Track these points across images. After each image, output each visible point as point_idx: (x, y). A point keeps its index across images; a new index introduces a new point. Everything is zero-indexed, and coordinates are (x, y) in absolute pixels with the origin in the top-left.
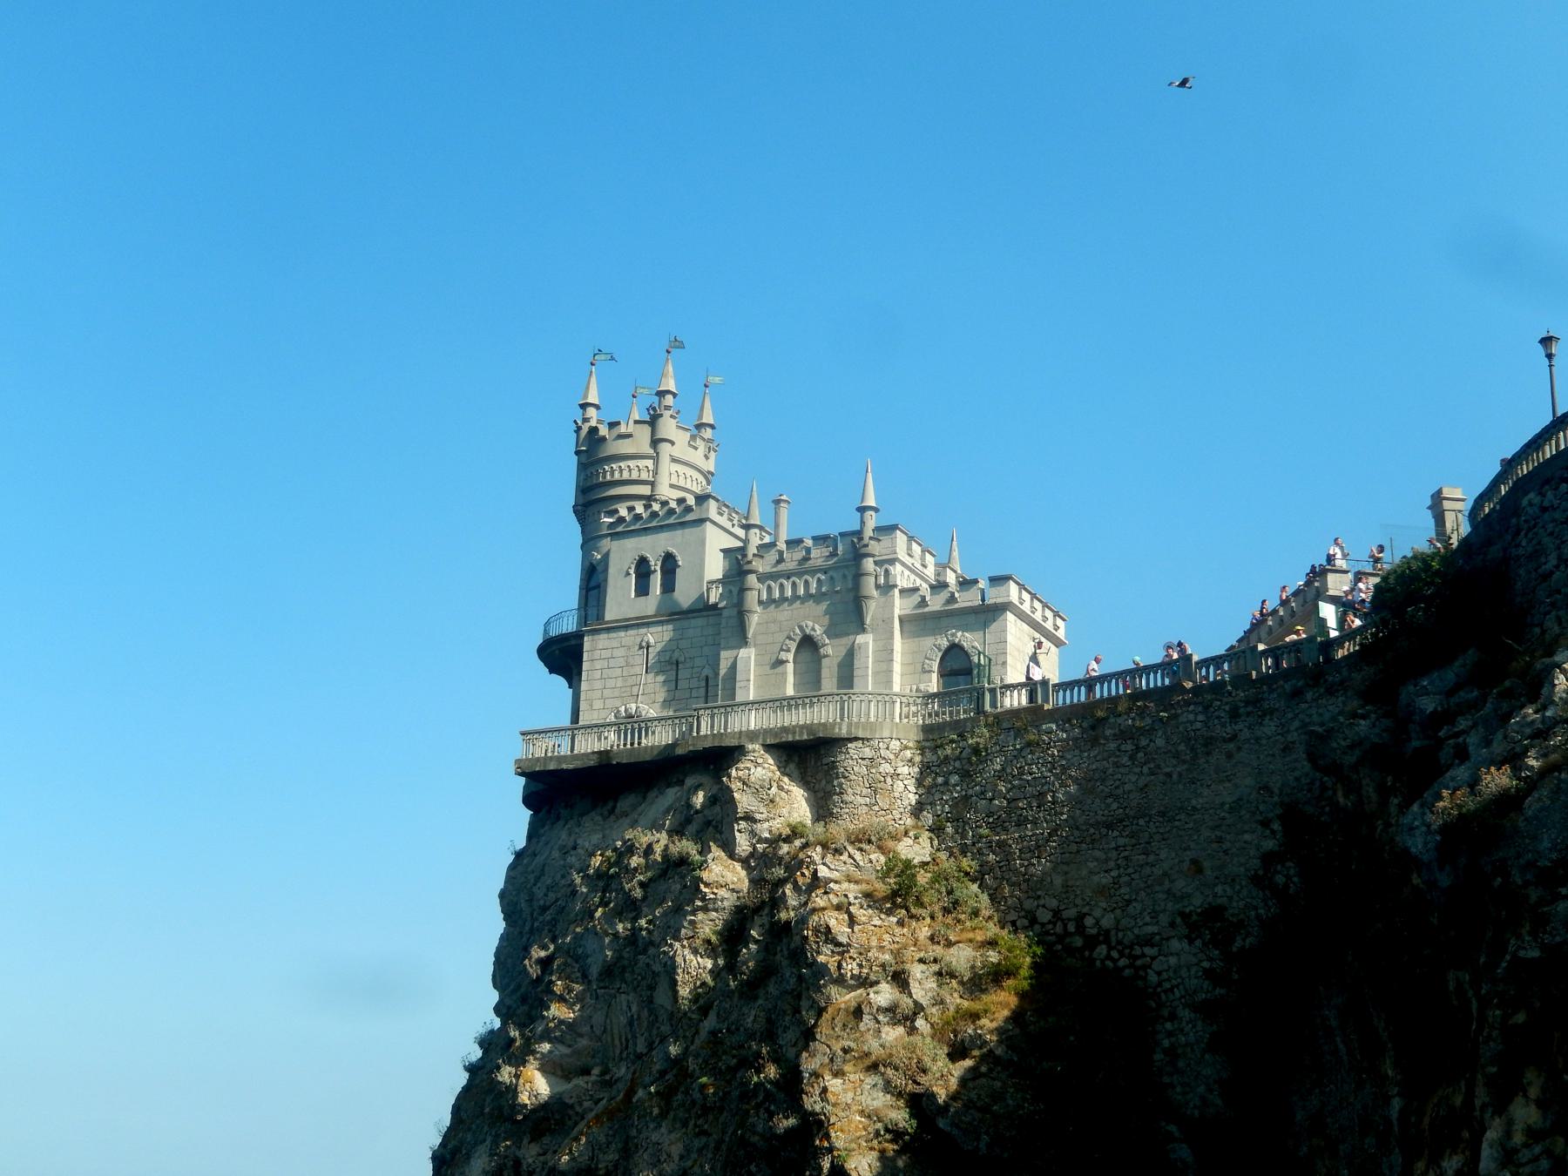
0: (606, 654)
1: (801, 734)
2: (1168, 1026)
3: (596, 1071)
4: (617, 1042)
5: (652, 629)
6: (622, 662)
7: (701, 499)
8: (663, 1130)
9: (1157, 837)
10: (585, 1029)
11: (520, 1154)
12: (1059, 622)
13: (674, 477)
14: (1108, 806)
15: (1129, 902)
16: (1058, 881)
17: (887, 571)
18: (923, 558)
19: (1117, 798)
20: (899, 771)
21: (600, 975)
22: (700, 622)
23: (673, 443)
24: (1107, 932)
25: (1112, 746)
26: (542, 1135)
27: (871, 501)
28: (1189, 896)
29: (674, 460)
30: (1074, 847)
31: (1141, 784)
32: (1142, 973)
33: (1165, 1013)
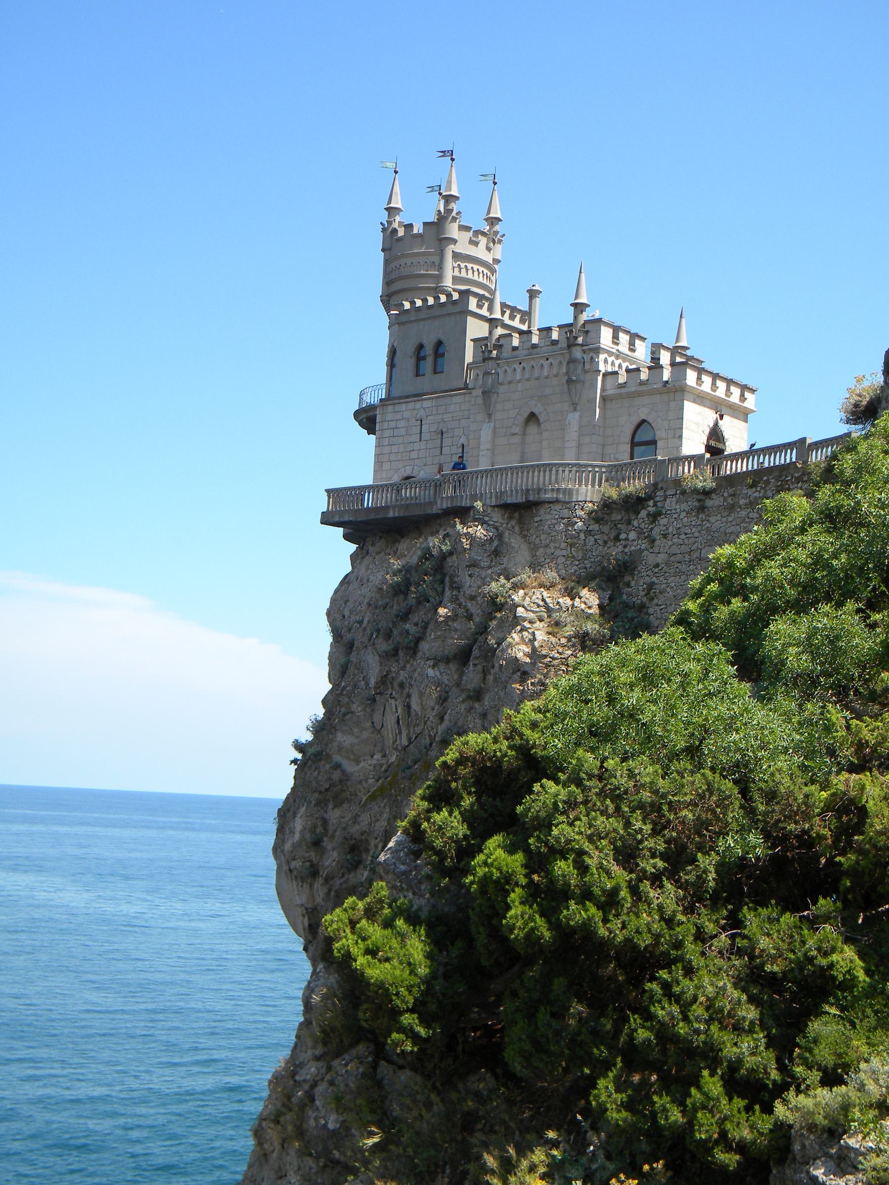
0: (392, 425)
1: (516, 498)
4: (390, 735)
5: (426, 404)
6: (403, 431)
7: (465, 294)
10: (369, 724)
11: (326, 816)
12: (747, 394)
13: (457, 270)
17: (592, 358)
18: (632, 344)
20: (591, 528)
23: (455, 241)
25: (743, 513)
26: (342, 803)
27: (583, 300)
29: (456, 256)
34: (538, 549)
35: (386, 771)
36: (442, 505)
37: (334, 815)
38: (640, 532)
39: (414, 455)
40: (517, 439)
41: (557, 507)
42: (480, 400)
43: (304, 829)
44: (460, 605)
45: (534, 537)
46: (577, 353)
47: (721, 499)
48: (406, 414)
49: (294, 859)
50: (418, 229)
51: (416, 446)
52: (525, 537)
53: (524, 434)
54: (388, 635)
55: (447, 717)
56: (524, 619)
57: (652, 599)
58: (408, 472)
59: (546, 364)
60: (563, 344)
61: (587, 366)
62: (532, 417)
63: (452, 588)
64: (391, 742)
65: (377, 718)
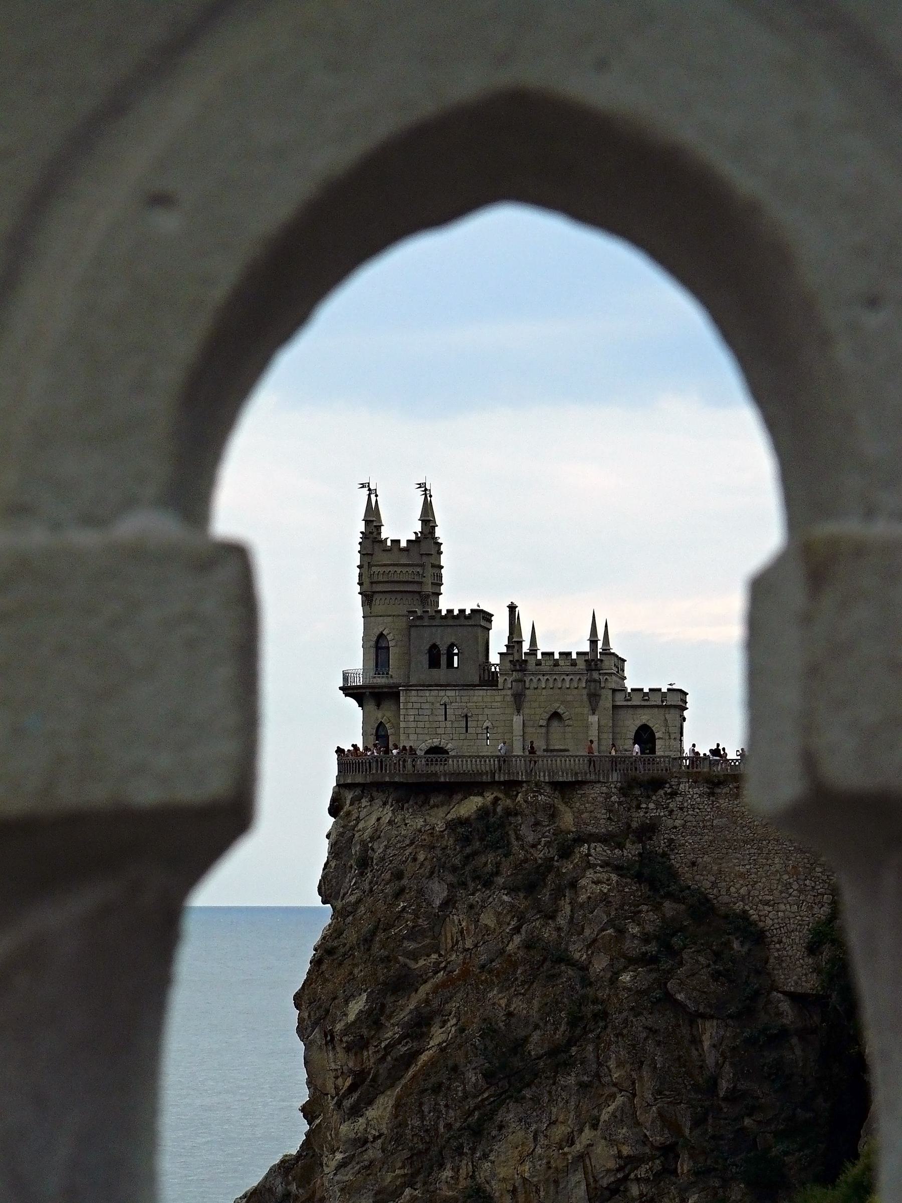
2: (778, 946)
3: (434, 956)
4: (449, 941)
5: (449, 693)
6: (428, 712)
8: (495, 992)
9: (773, 852)
14: (745, 831)
15: (756, 883)
16: (715, 868)
19: (749, 828)
21: (441, 904)
22: (481, 693)
24: (743, 896)
28: (790, 884)
30: (724, 851)
31: (764, 823)
32: (763, 918)
33: (776, 939)
34: (583, 813)
35: (445, 967)
36: (499, 777)
37: (389, 1000)
38: (658, 805)
39: (439, 731)
40: (543, 730)
41: (599, 785)
42: (509, 698)
43: (361, 1011)
44: (526, 851)
45: (578, 804)
46: (596, 675)
47: (728, 789)
48: (430, 699)
49: (346, 1035)
50: (403, 544)
51: (443, 724)
52: (566, 803)
53: (548, 725)
54: (454, 869)
55: (523, 930)
56: (595, 865)
57: (672, 850)
58: (436, 742)
59: (568, 679)
60: (582, 665)
61: (602, 685)
62: (556, 716)
63: (517, 839)
64: (450, 946)
65: (436, 929)
